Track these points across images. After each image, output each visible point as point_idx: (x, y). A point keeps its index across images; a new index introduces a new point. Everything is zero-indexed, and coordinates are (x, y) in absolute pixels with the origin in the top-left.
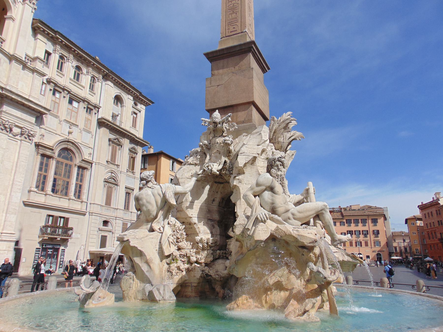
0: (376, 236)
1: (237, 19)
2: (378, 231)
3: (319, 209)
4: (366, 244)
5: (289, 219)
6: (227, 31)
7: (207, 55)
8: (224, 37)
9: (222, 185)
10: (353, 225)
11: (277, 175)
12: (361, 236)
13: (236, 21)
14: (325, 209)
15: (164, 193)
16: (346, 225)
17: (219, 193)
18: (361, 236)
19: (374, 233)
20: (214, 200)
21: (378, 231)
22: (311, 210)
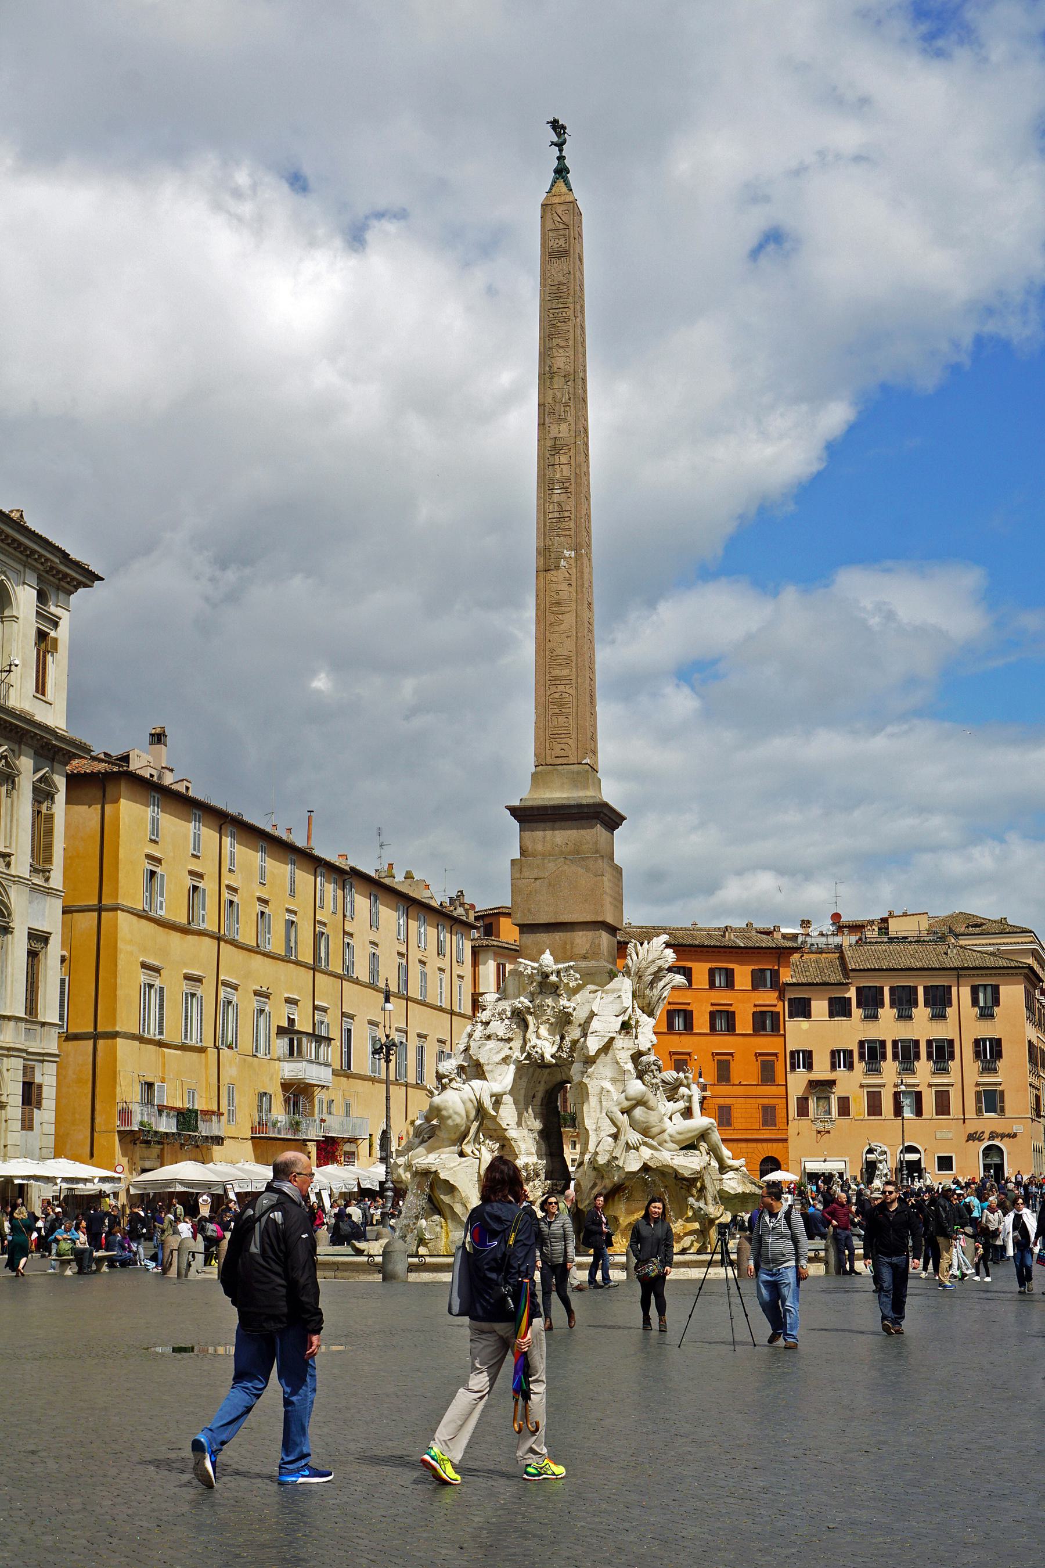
0: (986, 1065)
1: (568, 732)
2: (999, 1041)
3: (704, 1129)
4: (943, 1106)
5: (666, 1142)
6: (548, 752)
7: (514, 811)
8: (542, 765)
9: (548, 1070)
10: (887, 1013)
11: (652, 1084)
12: (924, 1066)
13: (567, 736)
14: (713, 1128)
15: (478, 1098)
16: (857, 1012)
17: (542, 1083)
18: (924, 1066)
19: (977, 1055)
20: (534, 1097)
21: (997, 1043)
22: (694, 1131)
